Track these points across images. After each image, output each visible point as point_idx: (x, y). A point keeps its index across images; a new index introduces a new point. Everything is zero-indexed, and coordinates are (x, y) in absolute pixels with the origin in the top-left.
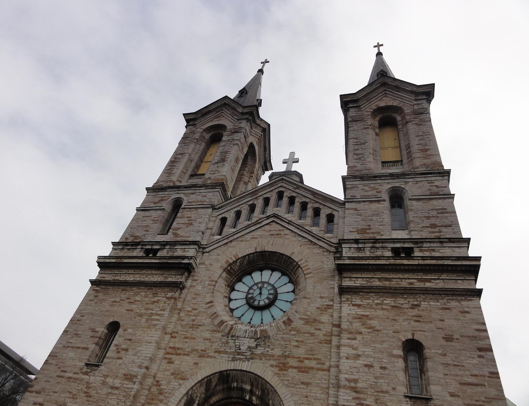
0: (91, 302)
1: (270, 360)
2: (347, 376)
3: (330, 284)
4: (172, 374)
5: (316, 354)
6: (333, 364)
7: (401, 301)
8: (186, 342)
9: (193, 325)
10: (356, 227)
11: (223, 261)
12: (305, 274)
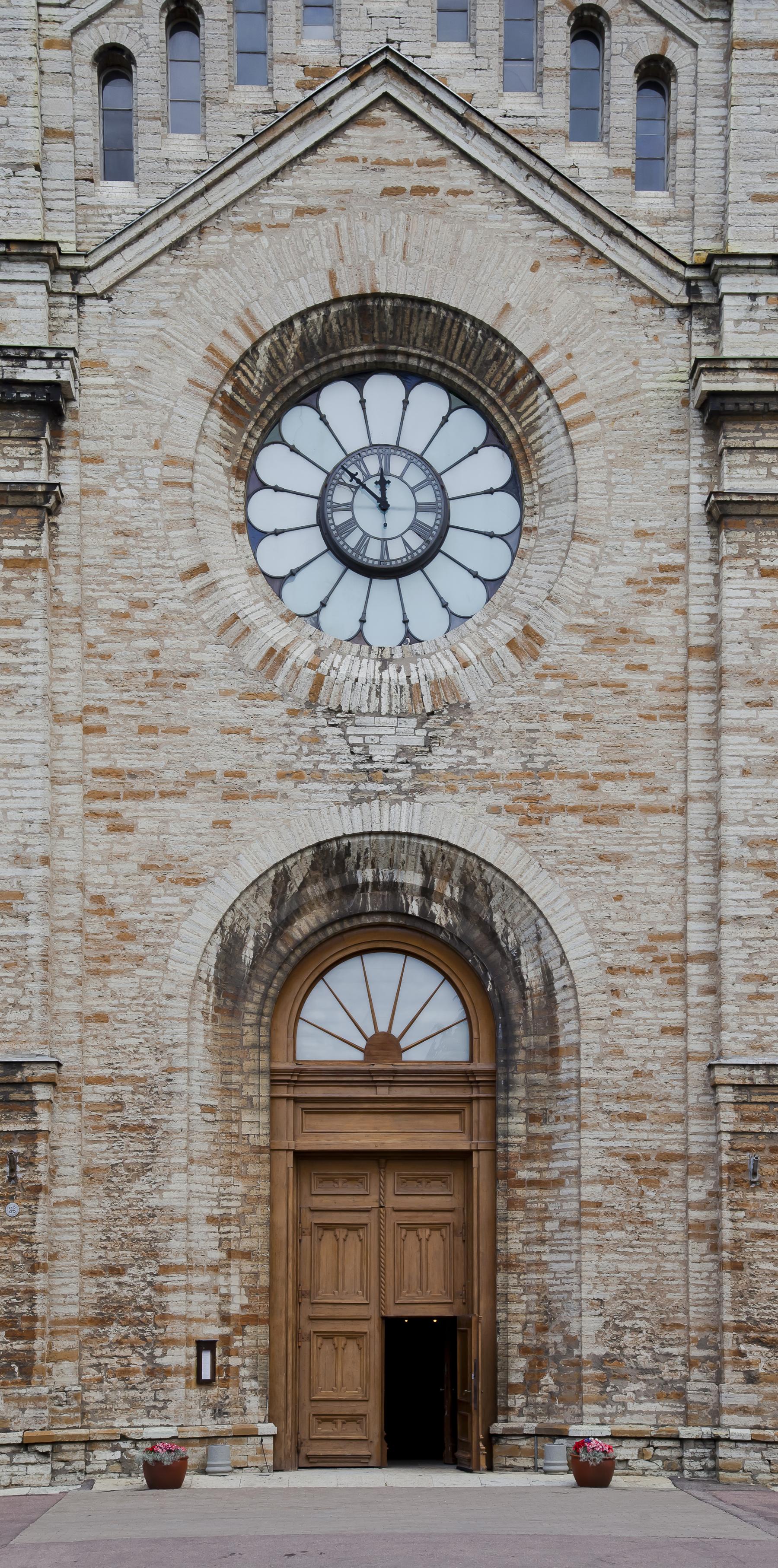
1: (483, 790)
2: (744, 830)
3: (671, 471)
4: (145, 868)
5: (636, 759)
6: (693, 788)
8: (155, 747)
9: (156, 673)
11: (197, 355)
12: (567, 426)
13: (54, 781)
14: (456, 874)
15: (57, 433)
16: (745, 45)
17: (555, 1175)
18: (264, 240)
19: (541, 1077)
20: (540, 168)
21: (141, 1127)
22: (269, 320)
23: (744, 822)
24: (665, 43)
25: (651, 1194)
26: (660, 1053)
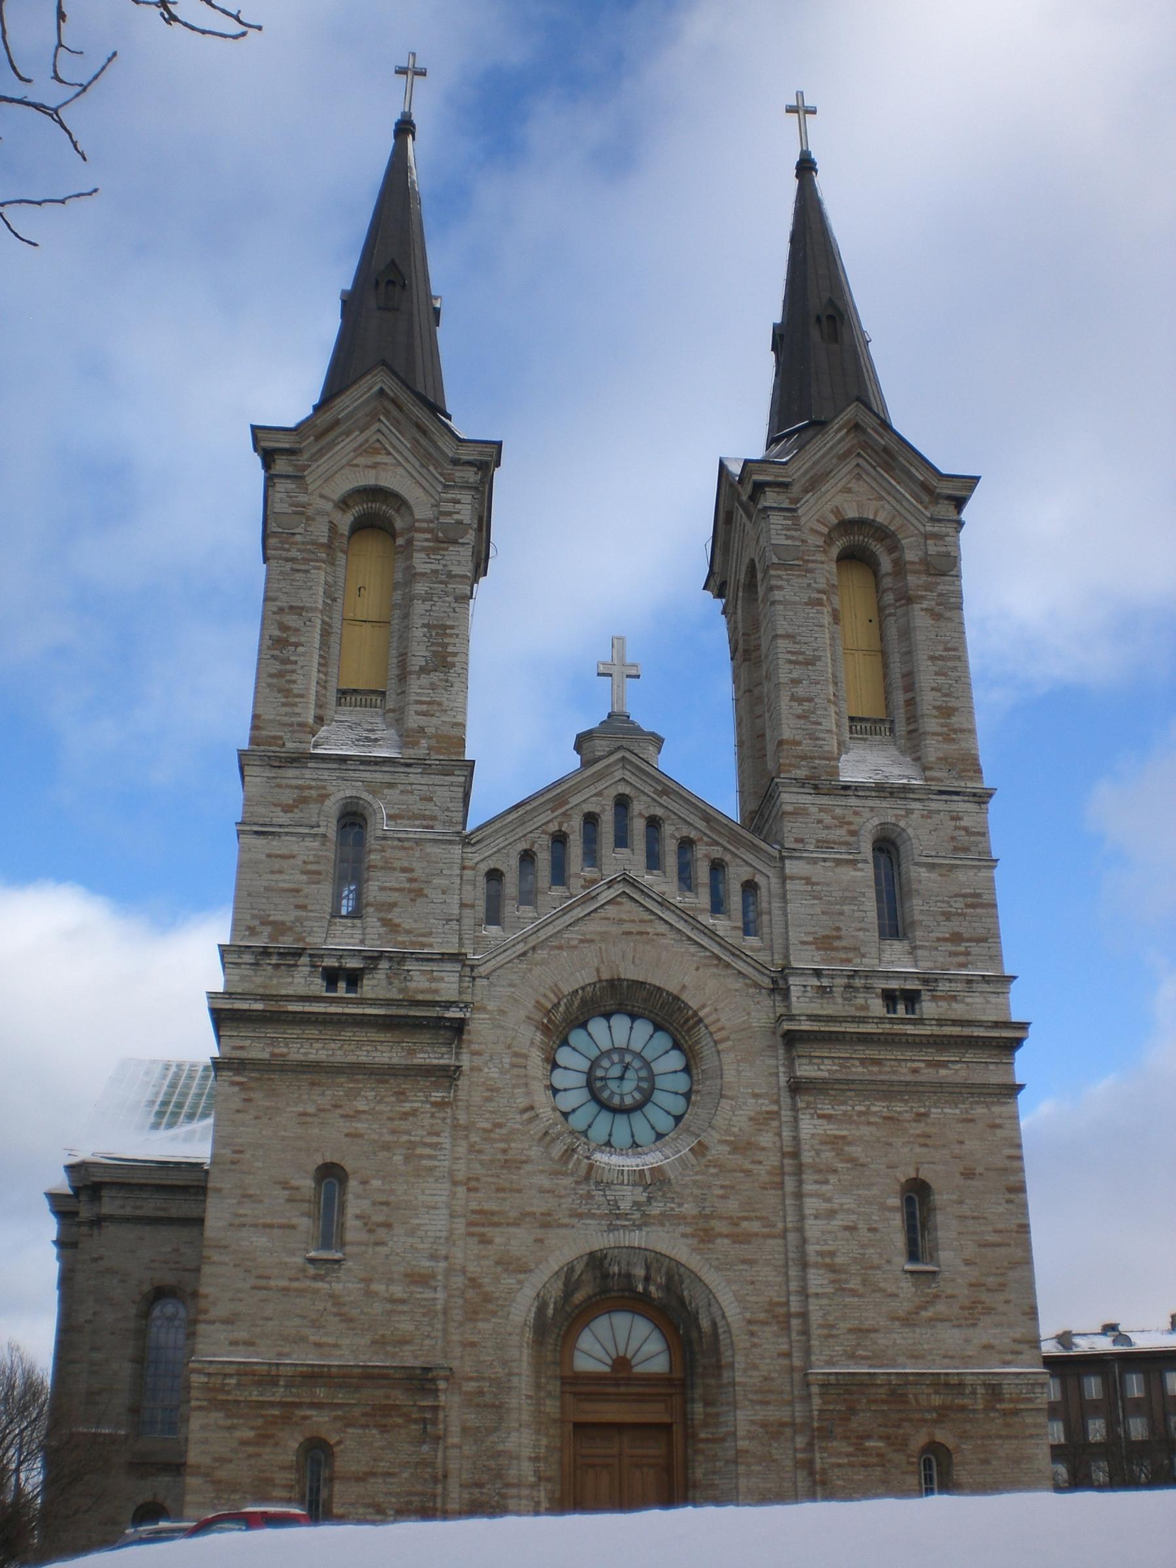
0: (240, 1115)
1: (679, 1224)
2: (818, 1248)
4: (498, 1263)
6: (789, 1225)
7: (899, 1107)
8: (504, 1199)
9: (506, 1161)
11: (530, 1005)
12: (716, 1043)
13: (452, 1216)
14: (663, 1271)
15: (460, 1040)
16: (792, 878)
17: (722, 1435)
18: (565, 954)
19: (712, 1382)
20: (698, 925)
21: (493, 1406)
22: (567, 989)
23: (818, 1244)
24: (754, 876)
25: (775, 1445)
26: (777, 1368)
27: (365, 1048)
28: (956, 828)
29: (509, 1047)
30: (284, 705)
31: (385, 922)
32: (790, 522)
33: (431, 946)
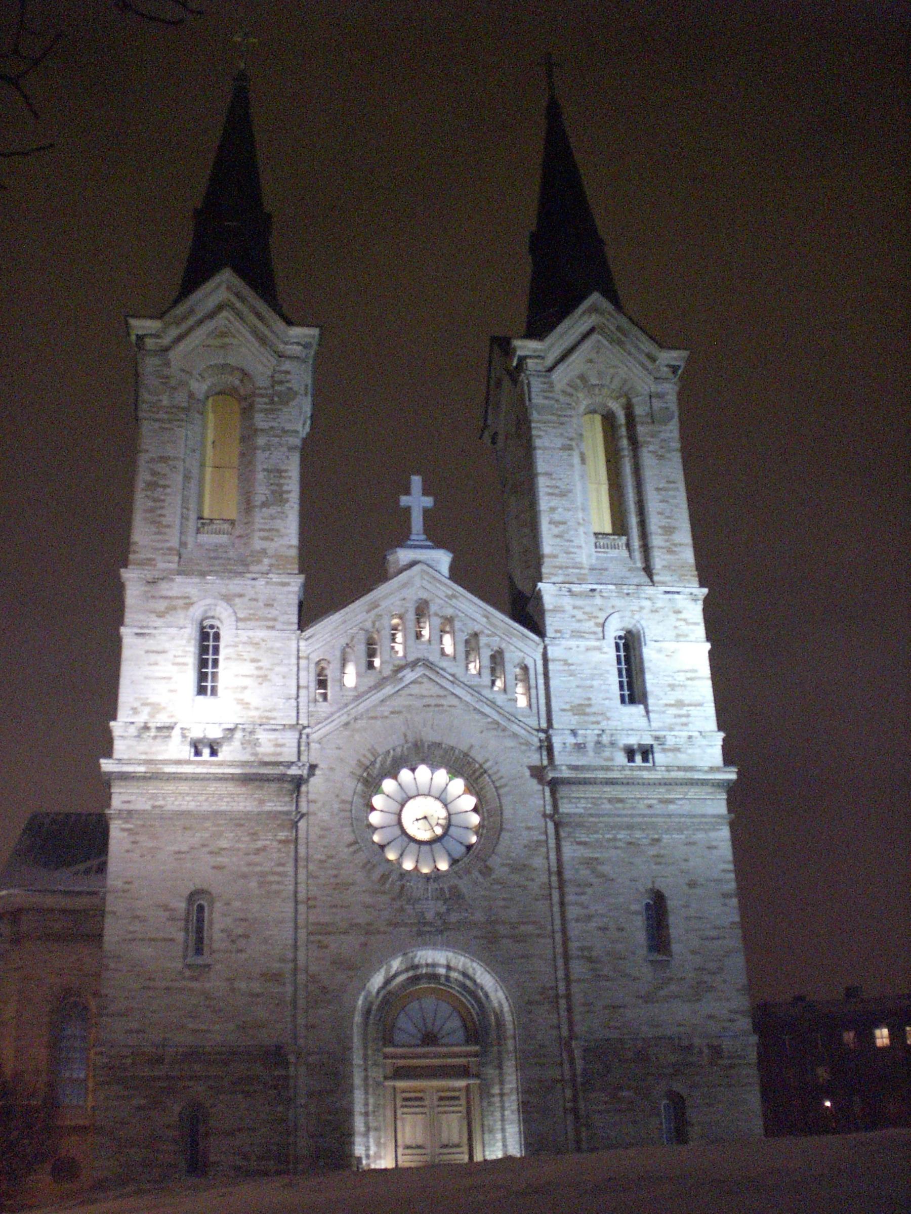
2: (578, 944)
9: (337, 884)
10: (568, 699)
20: (482, 698)
22: (381, 750)
27: (225, 800)
28: (678, 620)
29: (337, 796)
30: (155, 534)
31: (241, 702)
32: (545, 386)
33: (274, 719)
